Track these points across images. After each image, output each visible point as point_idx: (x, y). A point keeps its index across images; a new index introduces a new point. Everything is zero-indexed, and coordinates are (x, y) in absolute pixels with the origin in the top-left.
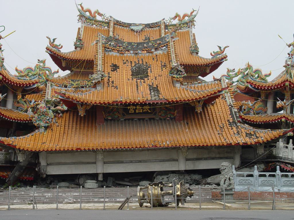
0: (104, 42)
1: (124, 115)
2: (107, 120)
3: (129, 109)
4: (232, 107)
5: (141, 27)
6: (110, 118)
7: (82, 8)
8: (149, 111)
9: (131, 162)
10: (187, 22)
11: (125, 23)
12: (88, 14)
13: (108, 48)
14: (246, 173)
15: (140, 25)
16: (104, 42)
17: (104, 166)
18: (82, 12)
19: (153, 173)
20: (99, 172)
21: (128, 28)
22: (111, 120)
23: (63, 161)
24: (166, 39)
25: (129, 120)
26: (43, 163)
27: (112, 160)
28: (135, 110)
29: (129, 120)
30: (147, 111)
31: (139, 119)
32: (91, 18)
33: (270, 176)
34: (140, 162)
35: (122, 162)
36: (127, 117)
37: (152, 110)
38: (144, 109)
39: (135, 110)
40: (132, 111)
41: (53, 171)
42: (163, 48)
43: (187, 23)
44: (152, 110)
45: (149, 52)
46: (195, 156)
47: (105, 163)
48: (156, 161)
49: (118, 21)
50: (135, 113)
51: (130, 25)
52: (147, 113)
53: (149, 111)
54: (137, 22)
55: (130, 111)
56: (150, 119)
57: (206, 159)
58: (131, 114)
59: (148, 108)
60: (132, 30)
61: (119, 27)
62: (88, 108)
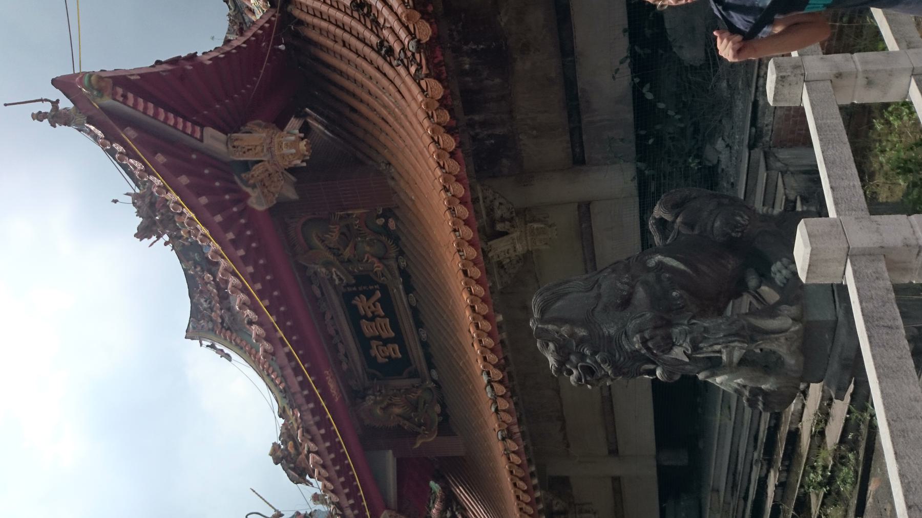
0: (210, 325)
3: (389, 357)
6: (438, 409)
8: (378, 294)
25: (429, 358)
28: (386, 342)
29: (429, 358)
30: (378, 305)
31: (419, 324)
37: (371, 287)
38: (373, 313)
39: (386, 342)
40: (394, 350)
44: (371, 287)
50: (399, 339)
52: (387, 303)
53: (378, 294)
55: (393, 355)
59: (368, 300)
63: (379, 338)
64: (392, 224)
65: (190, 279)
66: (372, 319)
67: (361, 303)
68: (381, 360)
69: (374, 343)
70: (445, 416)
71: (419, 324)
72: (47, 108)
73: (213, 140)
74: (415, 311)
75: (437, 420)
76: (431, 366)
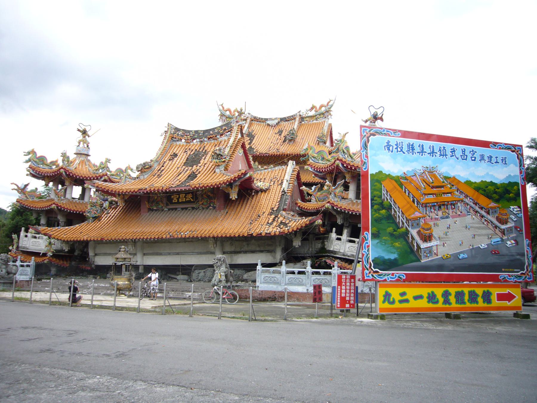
0: (172, 133)
1: (167, 205)
2: (150, 210)
3: (173, 199)
4: (285, 193)
5: (277, 121)
6: (155, 208)
7: (223, 108)
8: (192, 200)
9: (169, 254)
10: (324, 113)
11: (262, 119)
12: (228, 113)
13: (176, 138)
14: (296, 270)
15: (276, 119)
16: (172, 133)
17: (144, 258)
18: (223, 112)
19: (192, 266)
20: (138, 263)
21: (264, 123)
22: (156, 210)
23: (108, 252)
24: (232, 124)
25: (172, 209)
26: (91, 254)
27: (151, 252)
28: (178, 199)
29: (172, 209)
31: (183, 209)
32: (231, 116)
33: (325, 273)
34: (178, 254)
35: (161, 254)
36: (171, 207)
39: (178, 199)
41: (102, 261)
42: (228, 134)
43: (323, 114)
45: (214, 139)
46: (233, 249)
47: (144, 254)
48: (193, 253)
49: (255, 118)
50: (178, 203)
51: (266, 120)
53: (192, 200)
54: (273, 117)
56: (193, 208)
57: (246, 252)
58: (175, 203)
60: (268, 125)
61: (256, 122)
62: (126, 198)
63: (179, 197)
64: (211, 208)
65: (189, 132)
66: (185, 197)
68: (172, 197)
69: (178, 196)
70: (153, 210)
71: (183, 209)
72: (243, 111)
73: (238, 183)
74: (186, 209)
75: (151, 208)
76: (169, 210)
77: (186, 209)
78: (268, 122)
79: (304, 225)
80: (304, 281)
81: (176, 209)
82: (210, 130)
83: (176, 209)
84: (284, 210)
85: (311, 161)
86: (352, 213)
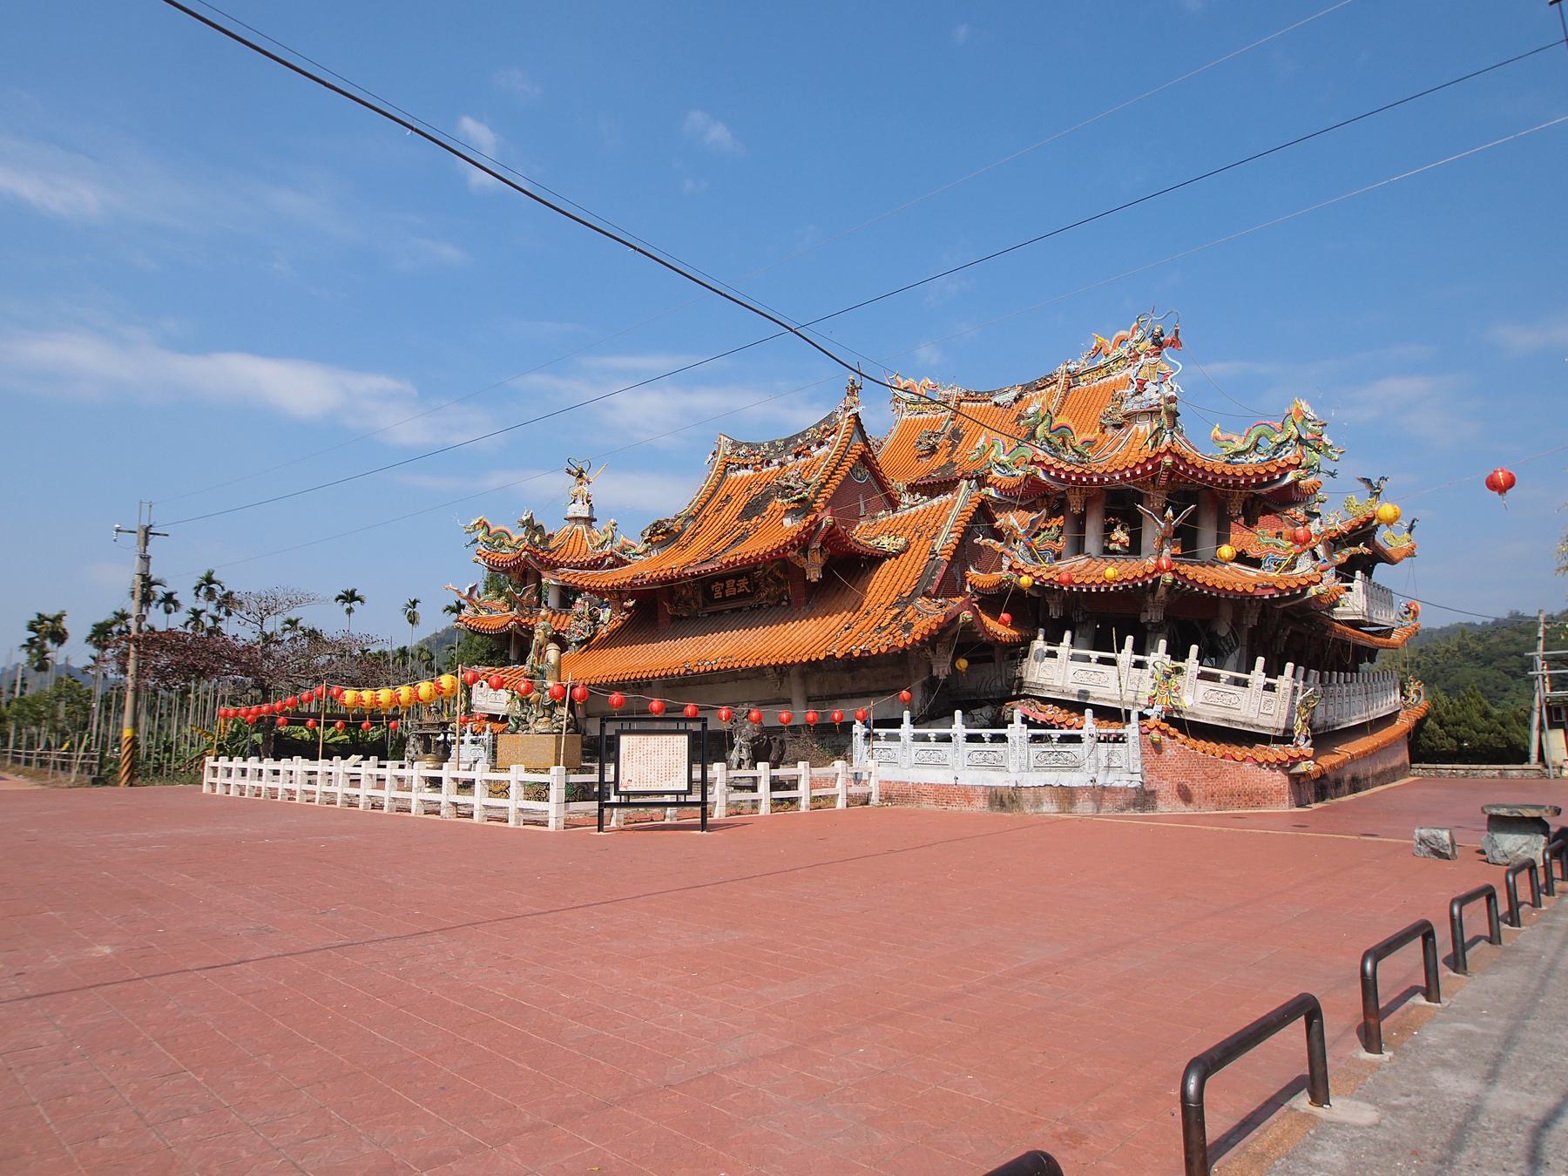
1: (705, 605)
25: (715, 613)
29: (715, 613)
31: (733, 610)
36: (711, 609)
50: (724, 599)
60: (996, 404)
67: (743, 582)
77: (739, 610)
78: (997, 399)
79: (934, 627)
80: (899, 754)
81: (721, 612)
82: (798, 436)
83: (721, 612)
84: (926, 594)
85: (995, 474)
86: (1098, 589)
